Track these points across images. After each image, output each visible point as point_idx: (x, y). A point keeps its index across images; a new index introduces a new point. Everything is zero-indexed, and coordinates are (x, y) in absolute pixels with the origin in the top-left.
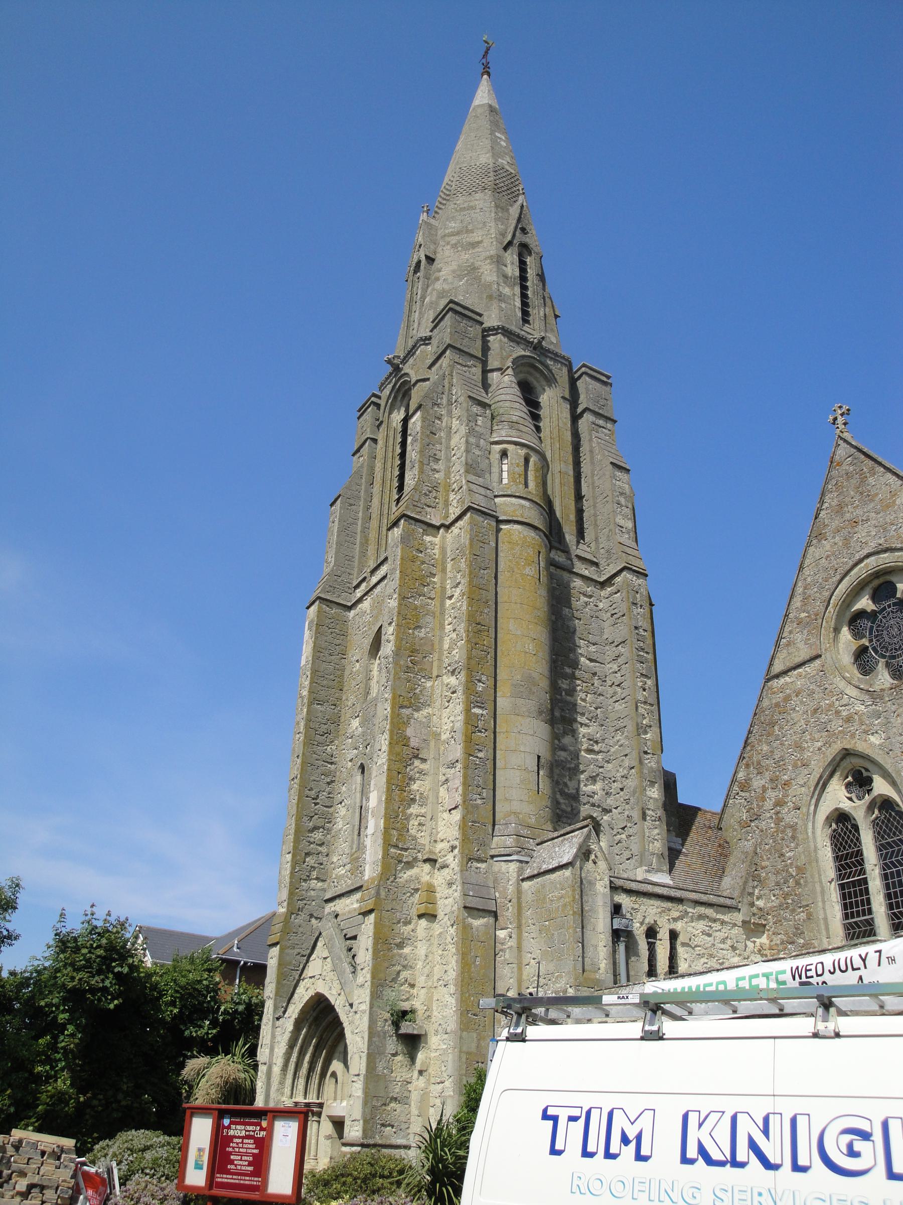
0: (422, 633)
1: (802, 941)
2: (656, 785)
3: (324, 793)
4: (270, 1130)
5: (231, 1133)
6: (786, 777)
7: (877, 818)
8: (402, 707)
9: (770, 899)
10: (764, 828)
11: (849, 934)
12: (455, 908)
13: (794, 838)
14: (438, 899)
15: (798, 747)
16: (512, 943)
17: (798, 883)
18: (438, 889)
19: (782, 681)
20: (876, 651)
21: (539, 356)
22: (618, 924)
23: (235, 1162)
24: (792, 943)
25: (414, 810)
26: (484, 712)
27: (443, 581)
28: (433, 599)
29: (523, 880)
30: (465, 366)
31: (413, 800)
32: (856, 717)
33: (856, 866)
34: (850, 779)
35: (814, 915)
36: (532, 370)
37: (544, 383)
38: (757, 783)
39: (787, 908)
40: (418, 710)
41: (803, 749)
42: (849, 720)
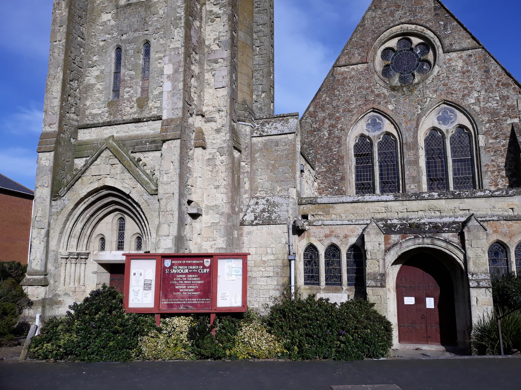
1: (337, 188)
3: (78, 58)
4: (213, 268)
5: (174, 271)
6: (338, 115)
7: (380, 141)
9: (321, 168)
10: (322, 136)
11: (358, 187)
12: (225, 145)
13: (338, 143)
14: (206, 139)
15: (348, 102)
17: (338, 162)
18: (205, 133)
19: (343, 69)
20: (394, 69)
23: (181, 290)
24: (332, 188)
29: (253, 137)
32: (382, 95)
33: (365, 160)
34: (370, 122)
35: (346, 177)
38: (321, 115)
39: (330, 173)
41: (349, 104)
42: (378, 96)
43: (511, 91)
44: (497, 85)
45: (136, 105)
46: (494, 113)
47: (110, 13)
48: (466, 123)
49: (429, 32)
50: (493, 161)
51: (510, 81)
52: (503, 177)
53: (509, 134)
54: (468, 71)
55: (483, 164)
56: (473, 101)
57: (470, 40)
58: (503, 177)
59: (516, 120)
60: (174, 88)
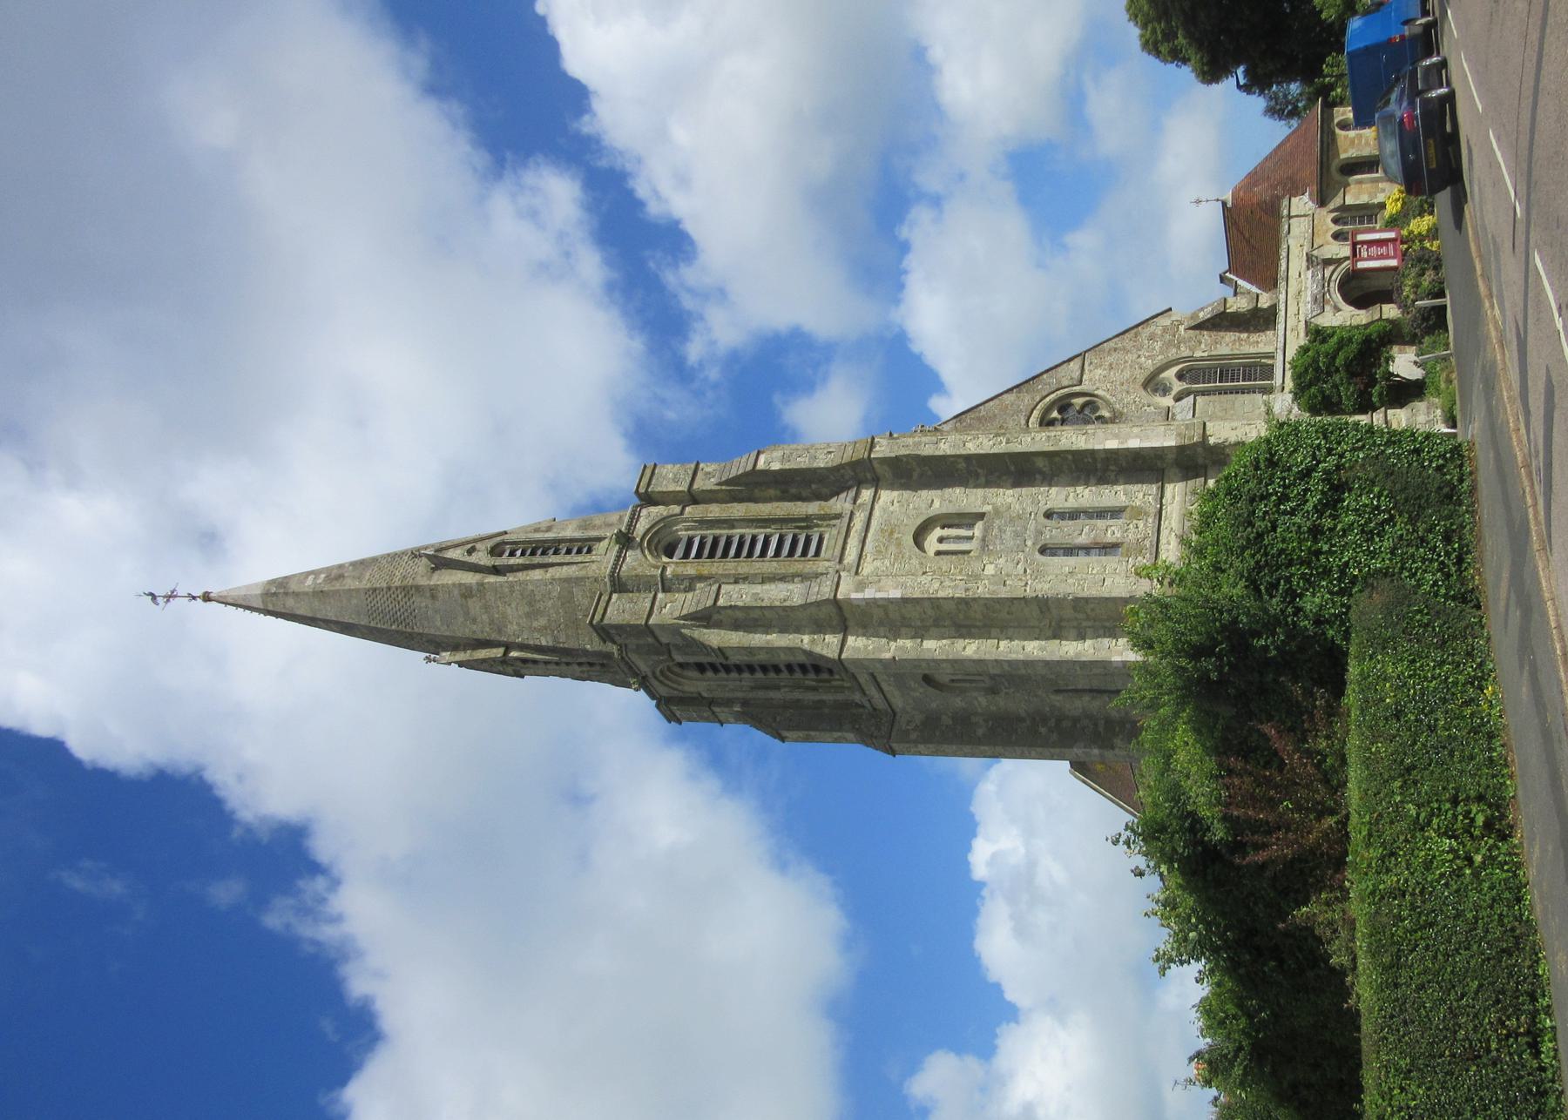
43: (1145, 331)
44: (1135, 341)
45: (1135, 522)
46: (1169, 344)
47: (984, 566)
48: (1175, 370)
49: (1048, 399)
50: (1227, 345)
51: (1133, 331)
52: (1248, 337)
53: (1198, 332)
54: (1111, 365)
55: (1231, 353)
56: (1150, 361)
57: (1072, 364)
58: (1248, 337)
59: (1182, 328)
60: (1137, 436)
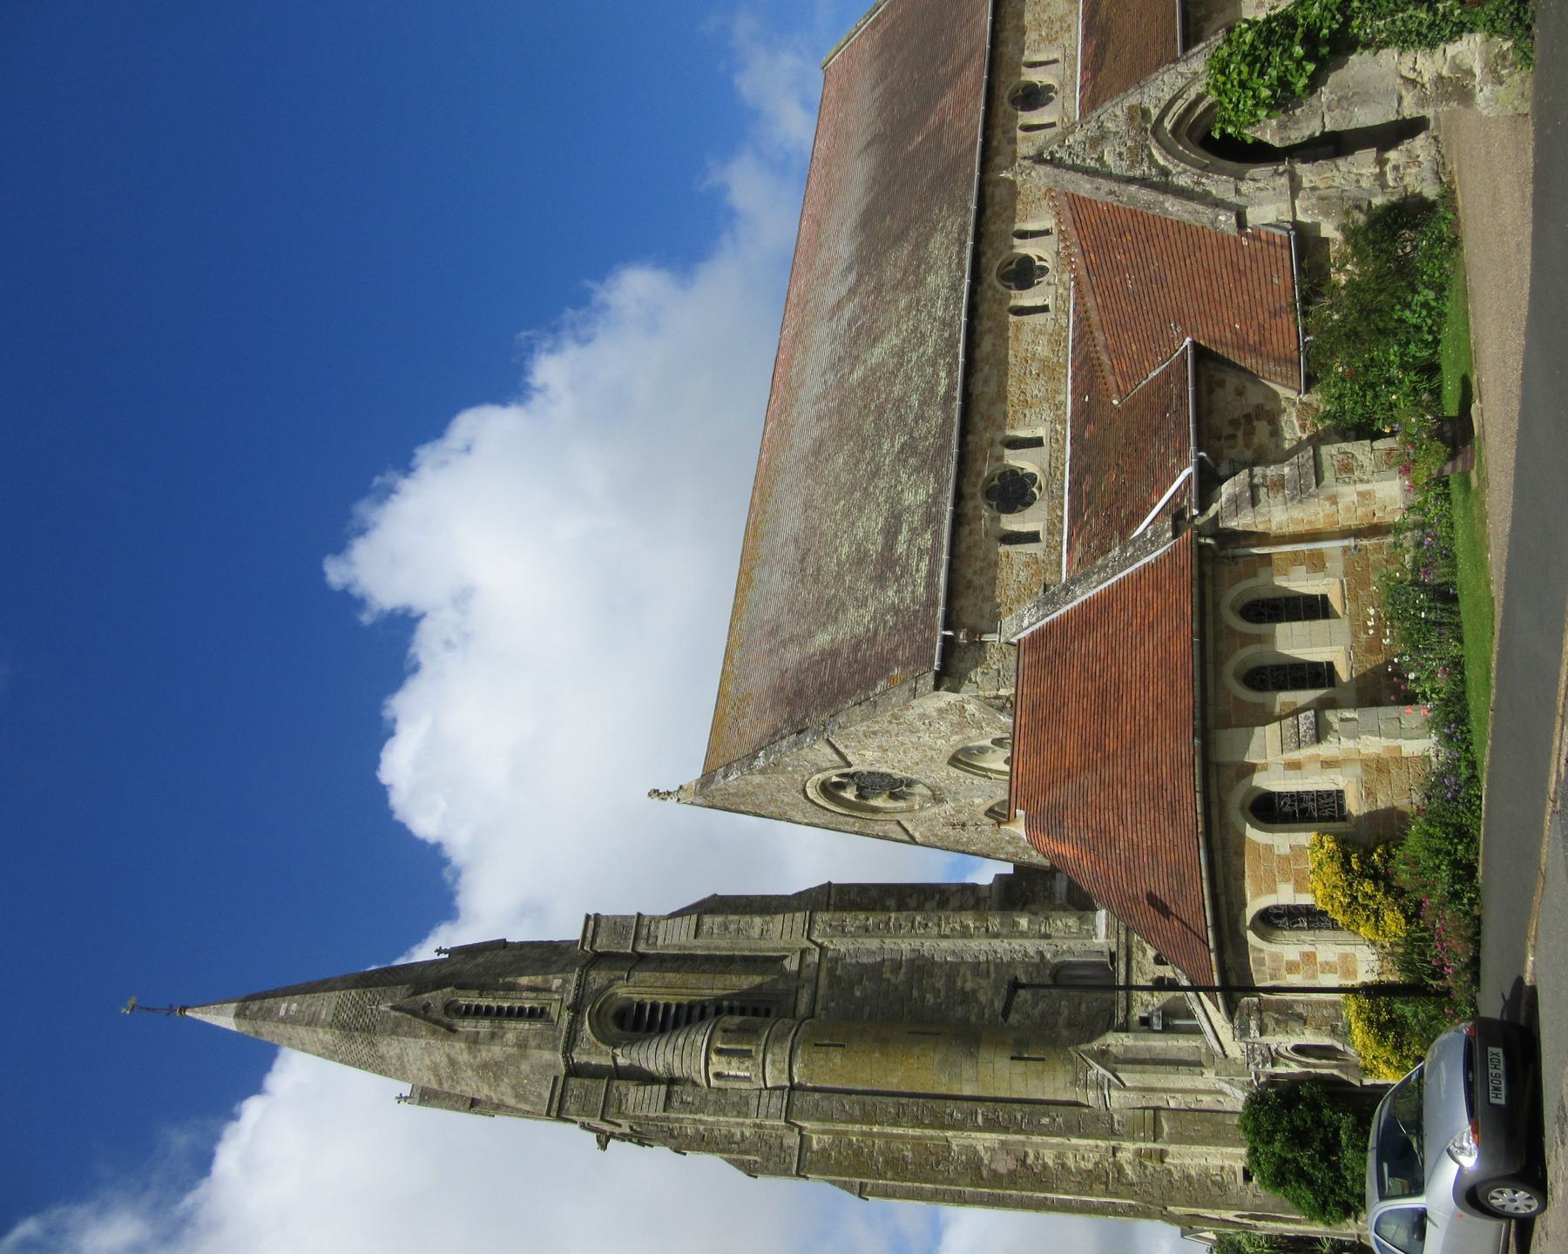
0: (909, 1154)
2: (1016, 919)
8: (982, 1178)
16: (1179, 1096)
21: (585, 1007)
22: (1157, 1024)
25: (1071, 1163)
26: (980, 1111)
27: (854, 1133)
28: (874, 1143)
30: (621, 1100)
31: (1063, 1165)
36: (602, 1012)
37: (614, 998)
40: (981, 1160)
